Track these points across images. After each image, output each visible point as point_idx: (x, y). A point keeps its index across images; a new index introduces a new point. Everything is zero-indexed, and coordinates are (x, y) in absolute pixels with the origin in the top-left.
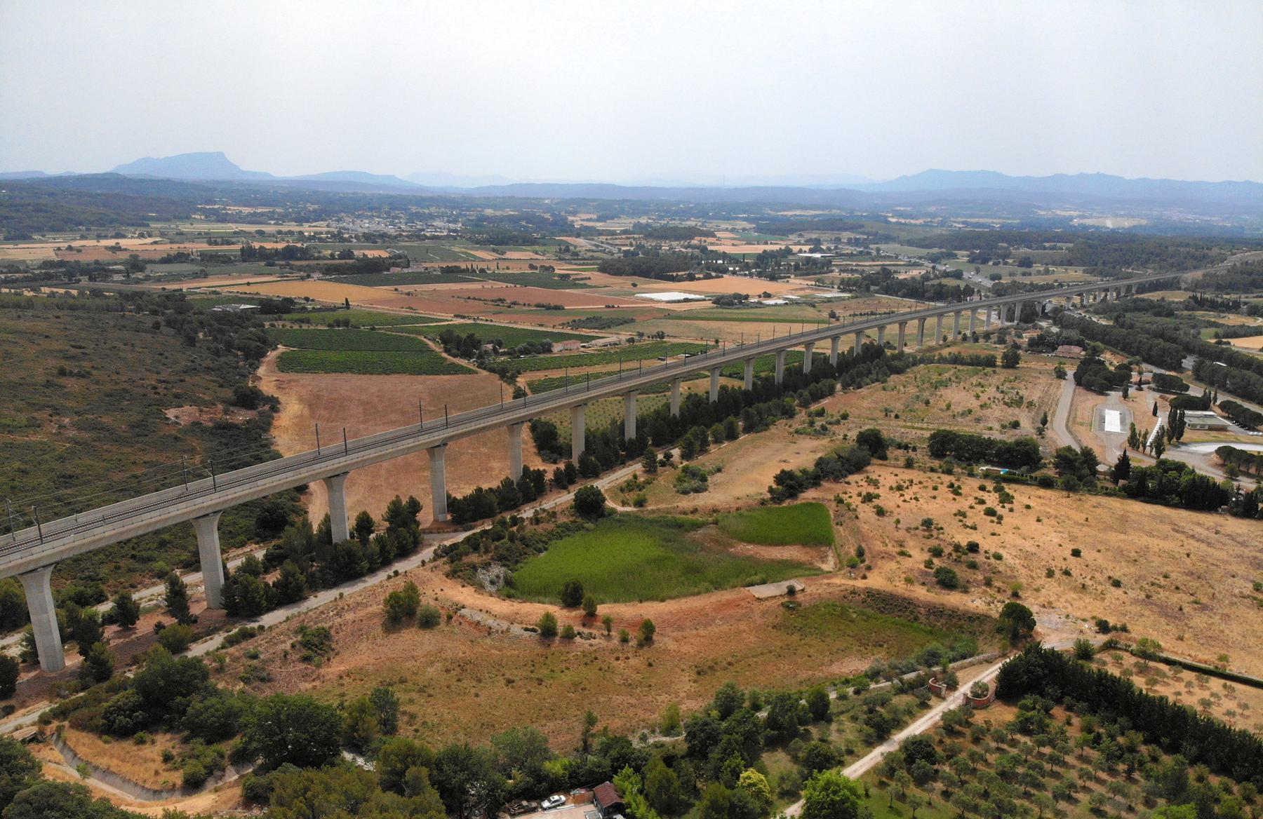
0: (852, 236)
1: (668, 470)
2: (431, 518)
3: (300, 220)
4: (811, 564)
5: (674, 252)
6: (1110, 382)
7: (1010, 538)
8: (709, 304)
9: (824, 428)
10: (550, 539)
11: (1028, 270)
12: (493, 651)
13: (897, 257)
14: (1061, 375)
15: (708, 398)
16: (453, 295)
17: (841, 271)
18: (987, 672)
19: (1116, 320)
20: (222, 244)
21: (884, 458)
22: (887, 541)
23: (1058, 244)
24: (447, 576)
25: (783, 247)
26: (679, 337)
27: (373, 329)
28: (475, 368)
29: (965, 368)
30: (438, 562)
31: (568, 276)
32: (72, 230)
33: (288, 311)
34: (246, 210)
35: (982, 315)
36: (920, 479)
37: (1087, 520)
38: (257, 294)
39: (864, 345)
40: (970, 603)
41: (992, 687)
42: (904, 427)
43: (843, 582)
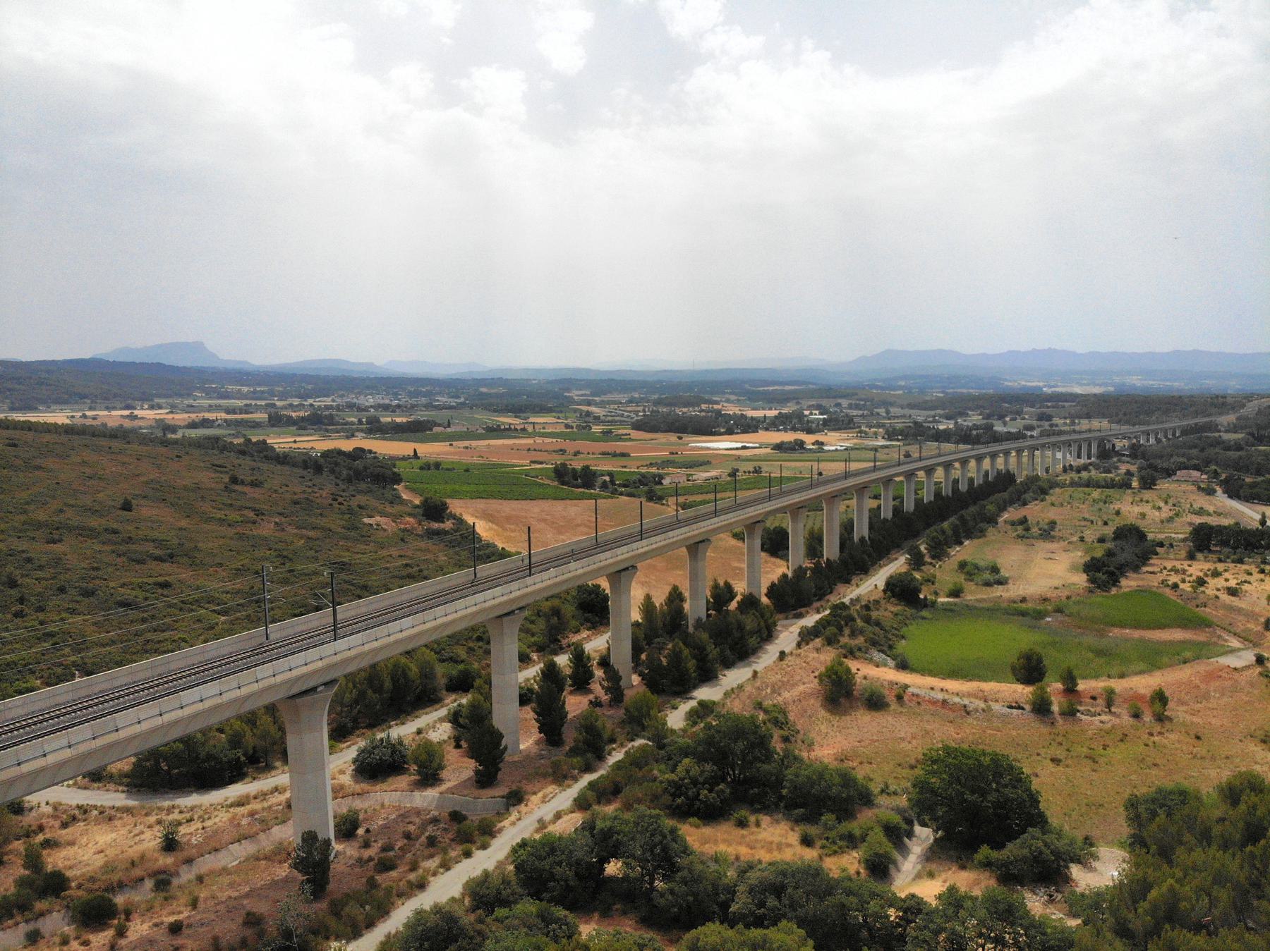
20: (240, 414)
32: (76, 403)
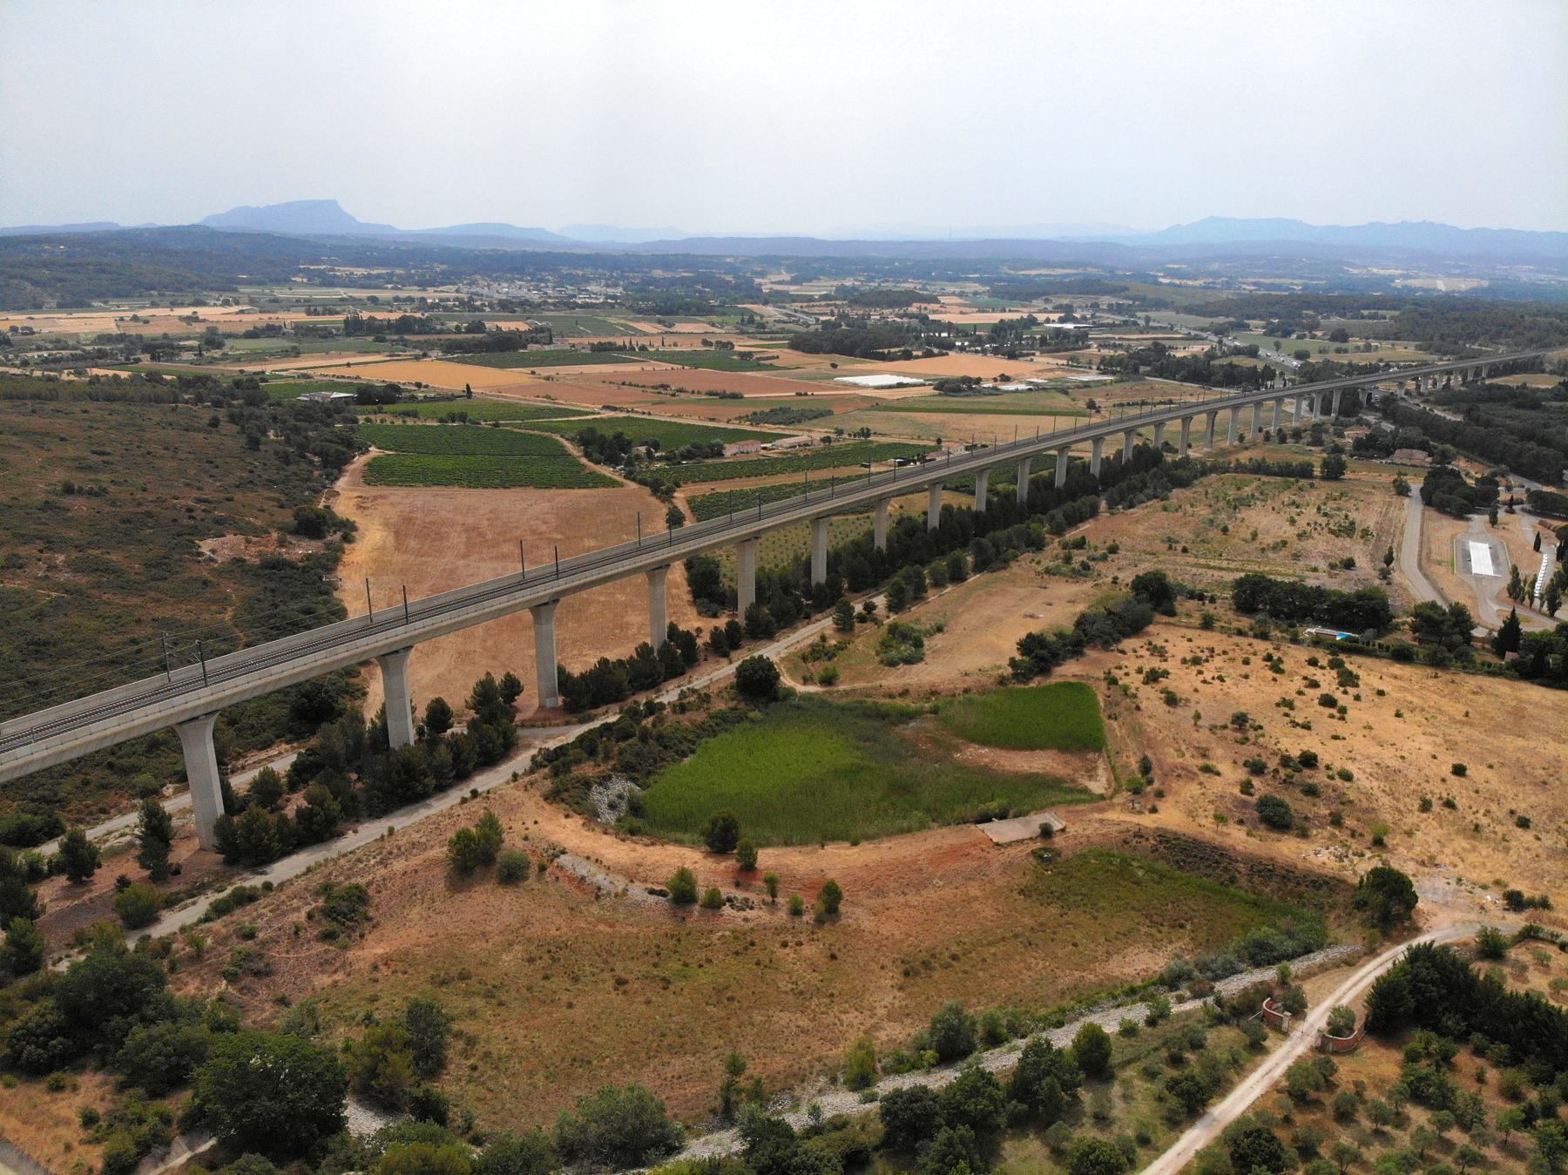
0: (1113, 301)
1: (869, 628)
2: (536, 702)
3: (423, 285)
4: (1073, 781)
5: (887, 323)
6: (1471, 501)
7: (1359, 743)
8: (929, 390)
9: (1085, 567)
10: (698, 737)
11: (1344, 346)
12: (601, 927)
13: (1172, 328)
14: (1402, 490)
15: (925, 523)
16: (605, 380)
17: (1100, 346)
18: (1349, 983)
19: (1468, 413)
20: (324, 314)
21: (1172, 613)
22: (1183, 748)
23: (1381, 312)
24: (546, 799)
25: (1025, 316)
26: (890, 435)
27: (496, 425)
28: (620, 479)
29: (1272, 479)
30: (536, 775)
31: (750, 354)
33: (392, 401)
34: (359, 272)
35: (1289, 407)
36: (1224, 646)
37: (1467, 714)
38: (358, 378)
39: (1135, 447)
40: (1312, 857)
41: (1361, 1014)
42: (1196, 565)
43: (1120, 817)
